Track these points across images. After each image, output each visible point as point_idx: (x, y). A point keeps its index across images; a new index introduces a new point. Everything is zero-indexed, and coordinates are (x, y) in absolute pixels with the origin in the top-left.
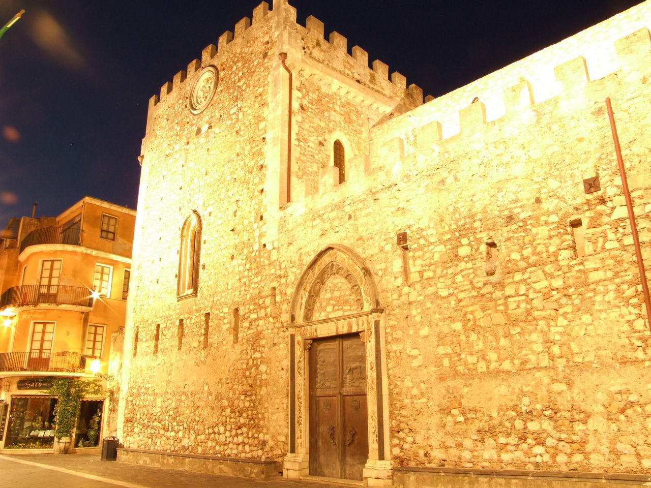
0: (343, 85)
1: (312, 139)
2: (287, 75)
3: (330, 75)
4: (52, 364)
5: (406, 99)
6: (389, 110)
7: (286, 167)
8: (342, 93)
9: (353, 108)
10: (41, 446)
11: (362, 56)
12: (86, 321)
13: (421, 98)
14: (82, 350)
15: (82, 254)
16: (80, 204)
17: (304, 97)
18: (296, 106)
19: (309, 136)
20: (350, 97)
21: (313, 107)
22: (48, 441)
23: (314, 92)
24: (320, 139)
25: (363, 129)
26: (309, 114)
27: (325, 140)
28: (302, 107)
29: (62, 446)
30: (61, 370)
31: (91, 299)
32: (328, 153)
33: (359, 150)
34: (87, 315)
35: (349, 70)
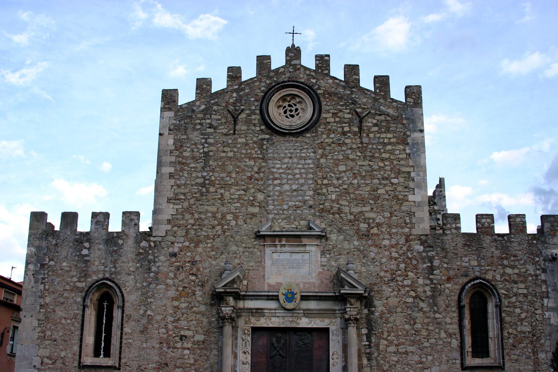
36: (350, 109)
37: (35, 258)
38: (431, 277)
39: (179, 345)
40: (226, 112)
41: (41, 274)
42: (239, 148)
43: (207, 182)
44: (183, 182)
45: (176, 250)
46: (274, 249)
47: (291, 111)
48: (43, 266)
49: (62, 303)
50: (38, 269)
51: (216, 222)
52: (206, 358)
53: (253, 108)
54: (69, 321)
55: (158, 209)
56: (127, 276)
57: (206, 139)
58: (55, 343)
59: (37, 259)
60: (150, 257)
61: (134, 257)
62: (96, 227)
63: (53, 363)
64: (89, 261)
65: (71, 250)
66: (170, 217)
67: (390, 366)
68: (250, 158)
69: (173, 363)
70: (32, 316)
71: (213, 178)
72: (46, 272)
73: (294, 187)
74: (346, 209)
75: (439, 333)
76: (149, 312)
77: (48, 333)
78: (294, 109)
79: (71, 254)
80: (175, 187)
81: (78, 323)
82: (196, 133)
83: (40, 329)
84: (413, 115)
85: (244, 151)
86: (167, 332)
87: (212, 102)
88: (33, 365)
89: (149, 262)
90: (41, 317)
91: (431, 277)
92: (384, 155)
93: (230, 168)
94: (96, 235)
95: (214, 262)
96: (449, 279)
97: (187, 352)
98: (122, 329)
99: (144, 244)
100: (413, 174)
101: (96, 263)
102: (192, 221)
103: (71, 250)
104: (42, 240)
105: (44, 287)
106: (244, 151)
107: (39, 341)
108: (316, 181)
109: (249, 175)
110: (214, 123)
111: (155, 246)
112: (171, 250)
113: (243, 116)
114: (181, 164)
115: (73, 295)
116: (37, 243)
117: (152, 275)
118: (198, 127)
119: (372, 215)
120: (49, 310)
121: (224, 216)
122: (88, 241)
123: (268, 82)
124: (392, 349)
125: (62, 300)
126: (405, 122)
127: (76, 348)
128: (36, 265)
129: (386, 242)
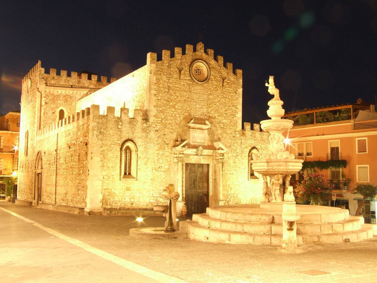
0: (63, 91)
1: (50, 112)
2: (40, 94)
3: (57, 89)
4: (3, 173)
5: (97, 84)
6: (85, 92)
7: (39, 124)
8: (64, 92)
9: (69, 96)
10: (3, 199)
11: (74, 75)
12: (13, 157)
13: (106, 81)
14: (13, 167)
15: (10, 133)
16: (8, 114)
17: (47, 99)
18: (43, 103)
19: (49, 112)
20: (67, 93)
21: (51, 102)
22: (4, 198)
23: (51, 96)
24: (53, 111)
25: (73, 102)
26: (49, 104)
27: (55, 111)
28: (46, 103)
29: (8, 199)
30: (5, 175)
31: (14, 150)
32: (56, 115)
33: (70, 110)
34: (14, 155)
35: (68, 82)
36: (220, 76)
37: (97, 128)
38: (241, 146)
39: (159, 170)
40: (177, 69)
41: (100, 136)
42: (181, 86)
43: (169, 100)
44: (159, 98)
45: (157, 129)
46: (193, 132)
47: (198, 72)
48: (100, 132)
49: (111, 150)
50: (98, 133)
51: (173, 118)
52: (169, 175)
53: (187, 69)
54: (114, 159)
55: (150, 109)
56: (138, 139)
57: (169, 81)
58: (109, 169)
59: (98, 129)
60: (148, 131)
61: (141, 130)
62: (124, 115)
63: (108, 178)
64: (122, 131)
65: (114, 126)
66: (155, 114)
67: (228, 179)
68: (185, 91)
69: (157, 177)
70: (97, 156)
71: (171, 99)
72: (102, 135)
73: (200, 106)
74: (217, 118)
75: (242, 167)
76: (147, 156)
77: (105, 164)
78: (199, 71)
79: (114, 127)
80: (156, 101)
81: (118, 159)
82: (164, 76)
83: (101, 162)
84: (239, 82)
85: (183, 88)
86: (155, 164)
87: (171, 63)
88: (100, 179)
89: (147, 133)
90: (102, 156)
91: (241, 146)
92: (230, 97)
93: (178, 95)
94: (124, 119)
95: (172, 135)
96: (246, 147)
97: (162, 173)
98: (137, 163)
99: (145, 125)
100: (238, 106)
101: (125, 132)
102: (163, 117)
103: (114, 126)
104: (100, 119)
105: (102, 142)
106: (183, 88)
107: (101, 168)
108: (208, 105)
109: (185, 99)
110: (172, 73)
111: (149, 126)
112: (156, 129)
113: (182, 72)
114: (159, 91)
115: (116, 147)
116: (97, 120)
117: (148, 139)
118: (165, 74)
119: (224, 121)
120: (105, 153)
121: (175, 116)
122: (121, 121)
123: (192, 58)
124: (229, 172)
125: (110, 149)
126: (236, 84)
127: (118, 171)
128: (97, 131)
129: (229, 132)
